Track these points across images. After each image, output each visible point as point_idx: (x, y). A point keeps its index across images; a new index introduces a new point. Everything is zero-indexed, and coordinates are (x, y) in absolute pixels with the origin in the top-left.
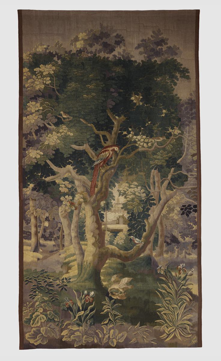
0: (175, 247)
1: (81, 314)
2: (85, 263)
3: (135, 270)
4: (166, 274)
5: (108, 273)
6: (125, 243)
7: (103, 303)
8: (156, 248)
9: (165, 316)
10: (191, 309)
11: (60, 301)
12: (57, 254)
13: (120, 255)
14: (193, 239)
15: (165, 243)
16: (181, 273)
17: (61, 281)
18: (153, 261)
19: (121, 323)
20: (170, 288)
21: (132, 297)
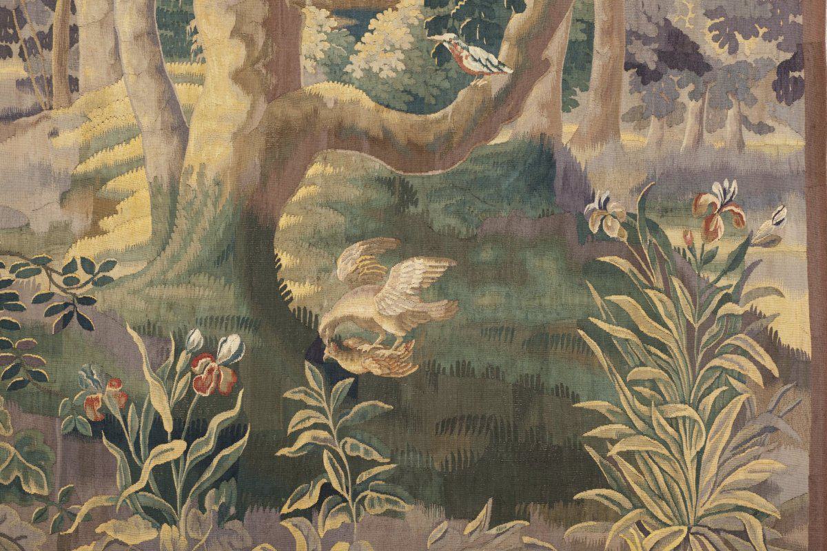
0: (684, 95)
1: (171, 457)
2: (193, 181)
3: (465, 220)
4: (634, 240)
5: (316, 232)
6: (409, 71)
7: (288, 395)
8: (581, 96)
9: (627, 469)
10: (775, 429)
11: (56, 387)
12: (39, 127)
13: (381, 136)
14: (779, 46)
15: (626, 69)
16: (716, 231)
17: (59, 280)
18: (565, 170)
19: (389, 507)
20: (656, 317)
21: (446, 364)
